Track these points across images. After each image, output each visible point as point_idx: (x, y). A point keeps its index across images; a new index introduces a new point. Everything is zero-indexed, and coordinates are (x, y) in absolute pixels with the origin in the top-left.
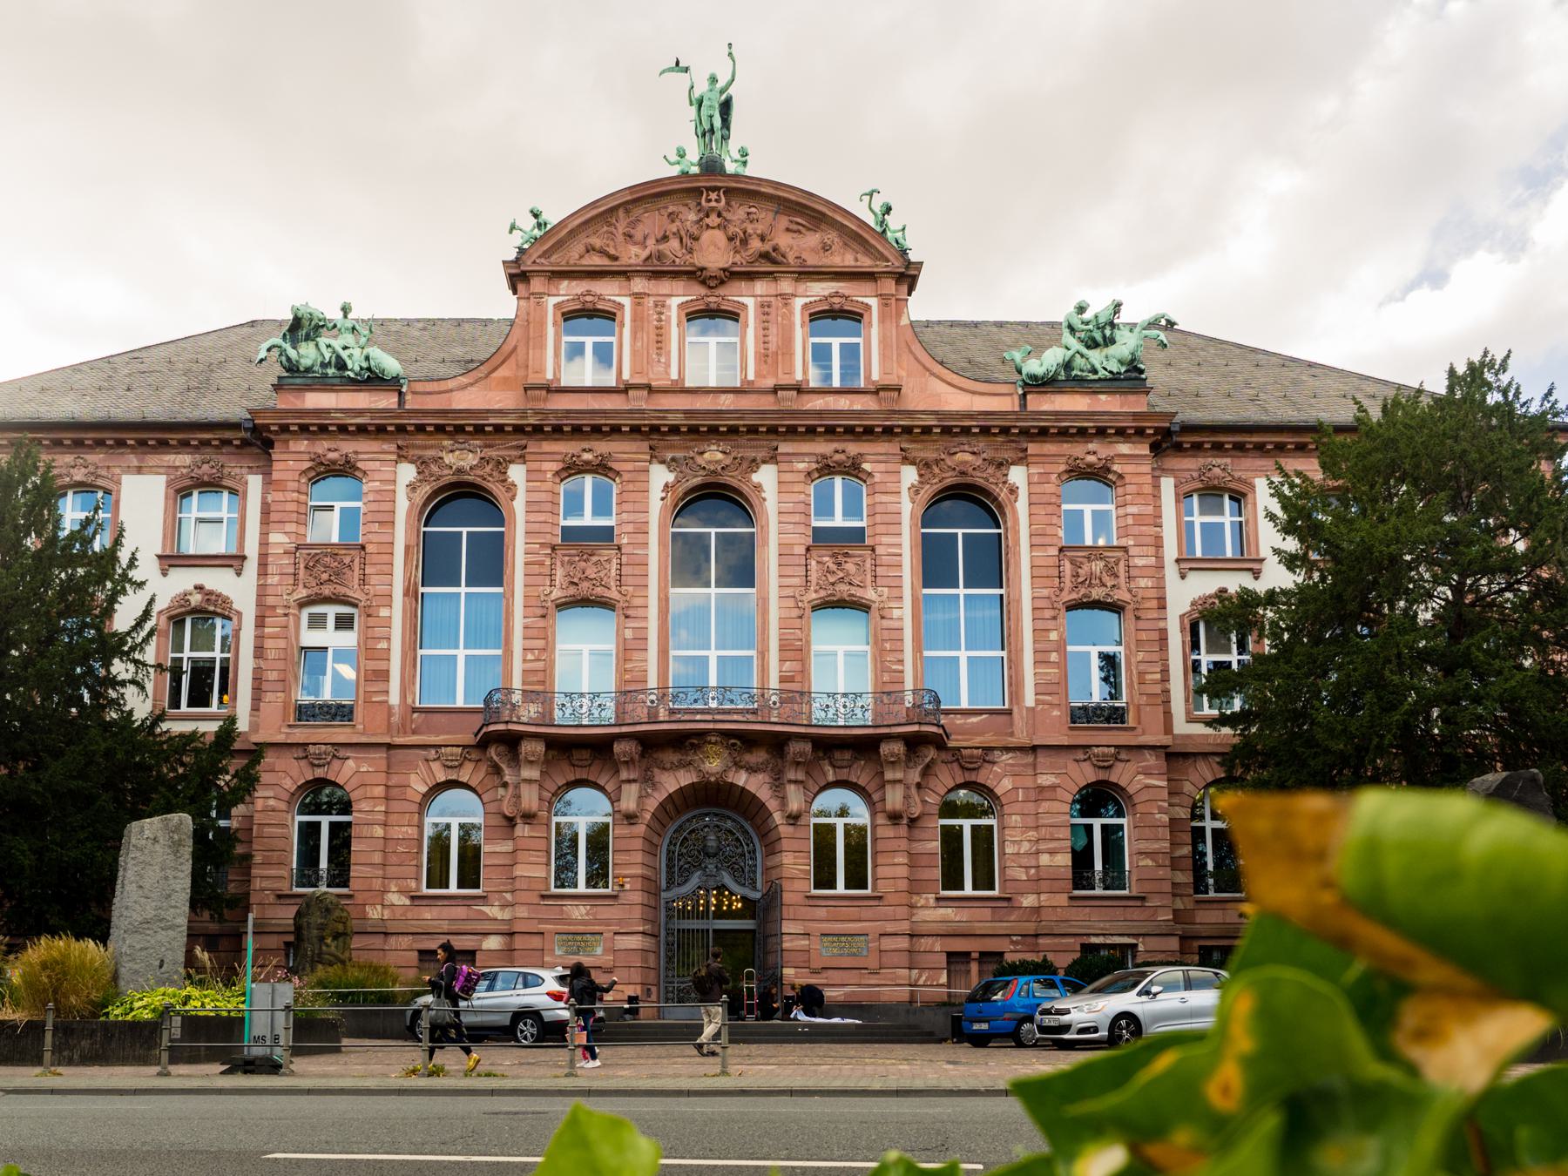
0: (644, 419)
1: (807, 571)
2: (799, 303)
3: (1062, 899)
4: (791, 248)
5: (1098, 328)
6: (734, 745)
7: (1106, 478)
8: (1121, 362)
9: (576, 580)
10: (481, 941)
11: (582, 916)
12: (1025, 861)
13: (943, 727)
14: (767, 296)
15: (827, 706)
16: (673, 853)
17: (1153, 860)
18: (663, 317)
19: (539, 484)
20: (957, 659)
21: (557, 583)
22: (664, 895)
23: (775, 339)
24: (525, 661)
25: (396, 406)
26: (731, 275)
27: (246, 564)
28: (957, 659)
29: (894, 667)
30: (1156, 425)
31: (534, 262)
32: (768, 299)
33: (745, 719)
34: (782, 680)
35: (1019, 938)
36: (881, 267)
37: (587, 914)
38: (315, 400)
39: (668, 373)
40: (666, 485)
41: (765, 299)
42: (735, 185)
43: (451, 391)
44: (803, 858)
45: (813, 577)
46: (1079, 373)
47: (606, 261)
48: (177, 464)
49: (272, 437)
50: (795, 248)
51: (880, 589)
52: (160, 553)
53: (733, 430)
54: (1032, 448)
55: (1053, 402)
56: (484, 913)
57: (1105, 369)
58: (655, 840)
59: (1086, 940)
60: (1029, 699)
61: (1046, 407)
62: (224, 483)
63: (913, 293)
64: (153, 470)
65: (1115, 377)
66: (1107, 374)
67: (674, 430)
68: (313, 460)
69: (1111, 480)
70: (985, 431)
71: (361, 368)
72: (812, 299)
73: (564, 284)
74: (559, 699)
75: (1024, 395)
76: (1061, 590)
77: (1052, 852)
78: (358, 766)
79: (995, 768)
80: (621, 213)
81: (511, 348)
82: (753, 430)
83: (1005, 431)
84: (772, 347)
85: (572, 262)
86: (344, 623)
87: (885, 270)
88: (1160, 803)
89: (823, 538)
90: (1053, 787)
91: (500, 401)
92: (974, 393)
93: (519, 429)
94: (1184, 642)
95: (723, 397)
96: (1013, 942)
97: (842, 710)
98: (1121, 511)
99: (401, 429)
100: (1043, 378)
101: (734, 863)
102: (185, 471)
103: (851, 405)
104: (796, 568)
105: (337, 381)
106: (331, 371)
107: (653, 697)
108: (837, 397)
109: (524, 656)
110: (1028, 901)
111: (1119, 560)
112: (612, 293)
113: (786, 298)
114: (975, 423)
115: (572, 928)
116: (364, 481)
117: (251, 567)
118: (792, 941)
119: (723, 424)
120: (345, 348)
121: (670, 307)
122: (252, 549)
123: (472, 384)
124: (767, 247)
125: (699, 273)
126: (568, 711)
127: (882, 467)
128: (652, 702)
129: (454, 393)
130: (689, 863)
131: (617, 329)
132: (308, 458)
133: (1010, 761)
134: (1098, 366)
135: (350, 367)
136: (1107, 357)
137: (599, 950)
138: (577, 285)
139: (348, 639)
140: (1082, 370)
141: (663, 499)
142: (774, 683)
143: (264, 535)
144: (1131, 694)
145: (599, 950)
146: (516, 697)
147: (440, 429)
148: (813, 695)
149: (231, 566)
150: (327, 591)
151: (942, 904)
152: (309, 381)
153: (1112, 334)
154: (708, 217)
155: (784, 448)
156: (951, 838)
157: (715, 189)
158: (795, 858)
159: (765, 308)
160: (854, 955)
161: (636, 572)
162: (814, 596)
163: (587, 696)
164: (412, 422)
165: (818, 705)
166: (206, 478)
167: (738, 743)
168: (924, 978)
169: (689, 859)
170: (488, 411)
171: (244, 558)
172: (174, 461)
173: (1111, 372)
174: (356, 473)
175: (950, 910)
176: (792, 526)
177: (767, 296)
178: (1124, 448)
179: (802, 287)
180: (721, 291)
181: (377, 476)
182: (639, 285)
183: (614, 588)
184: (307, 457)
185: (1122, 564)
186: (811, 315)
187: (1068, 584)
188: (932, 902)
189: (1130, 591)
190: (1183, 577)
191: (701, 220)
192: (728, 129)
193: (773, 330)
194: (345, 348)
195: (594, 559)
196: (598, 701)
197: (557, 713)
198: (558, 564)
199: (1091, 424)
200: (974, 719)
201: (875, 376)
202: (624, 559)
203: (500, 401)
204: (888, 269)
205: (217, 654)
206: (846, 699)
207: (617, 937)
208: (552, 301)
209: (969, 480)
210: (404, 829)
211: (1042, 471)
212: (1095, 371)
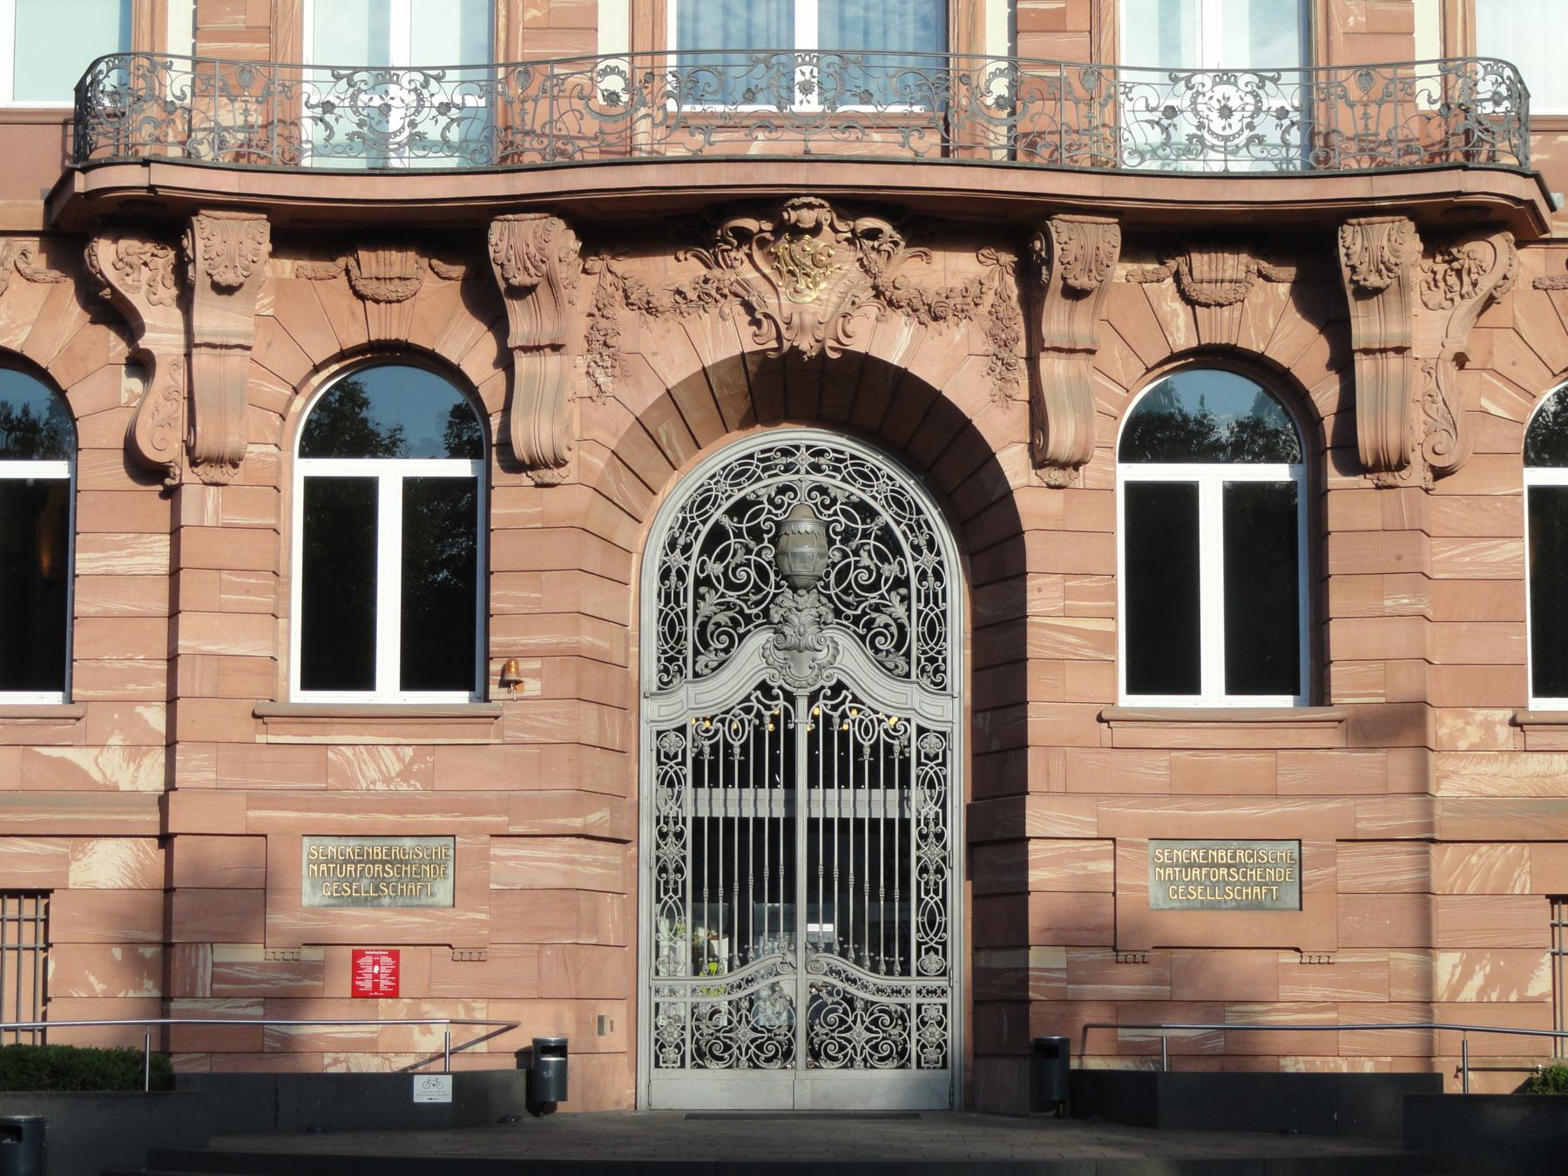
6: (873, 234)
10: (65, 861)
11: (387, 780)
13: (1537, 177)
15: (1171, 112)
16: (681, 576)
22: (650, 709)
33: (907, 154)
37: (405, 775)
44: (1093, 595)
56: (74, 769)
74: (315, 88)
97: (1217, 124)
101: (877, 608)
107: (615, 83)
115: (355, 819)
126: (345, 125)
128: (612, 97)
130: (728, 607)
137: (443, 891)
145: (443, 891)
146: (178, 82)
148: (1124, 76)
151: (1535, 738)
160: (1256, 906)
163: (405, 78)
165: (1141, 105)
167: (886, 228)
168: (1478, 980)
169: (732, 597)
196: (440, 93)
197: (310, 131)
206: (1228, 90)
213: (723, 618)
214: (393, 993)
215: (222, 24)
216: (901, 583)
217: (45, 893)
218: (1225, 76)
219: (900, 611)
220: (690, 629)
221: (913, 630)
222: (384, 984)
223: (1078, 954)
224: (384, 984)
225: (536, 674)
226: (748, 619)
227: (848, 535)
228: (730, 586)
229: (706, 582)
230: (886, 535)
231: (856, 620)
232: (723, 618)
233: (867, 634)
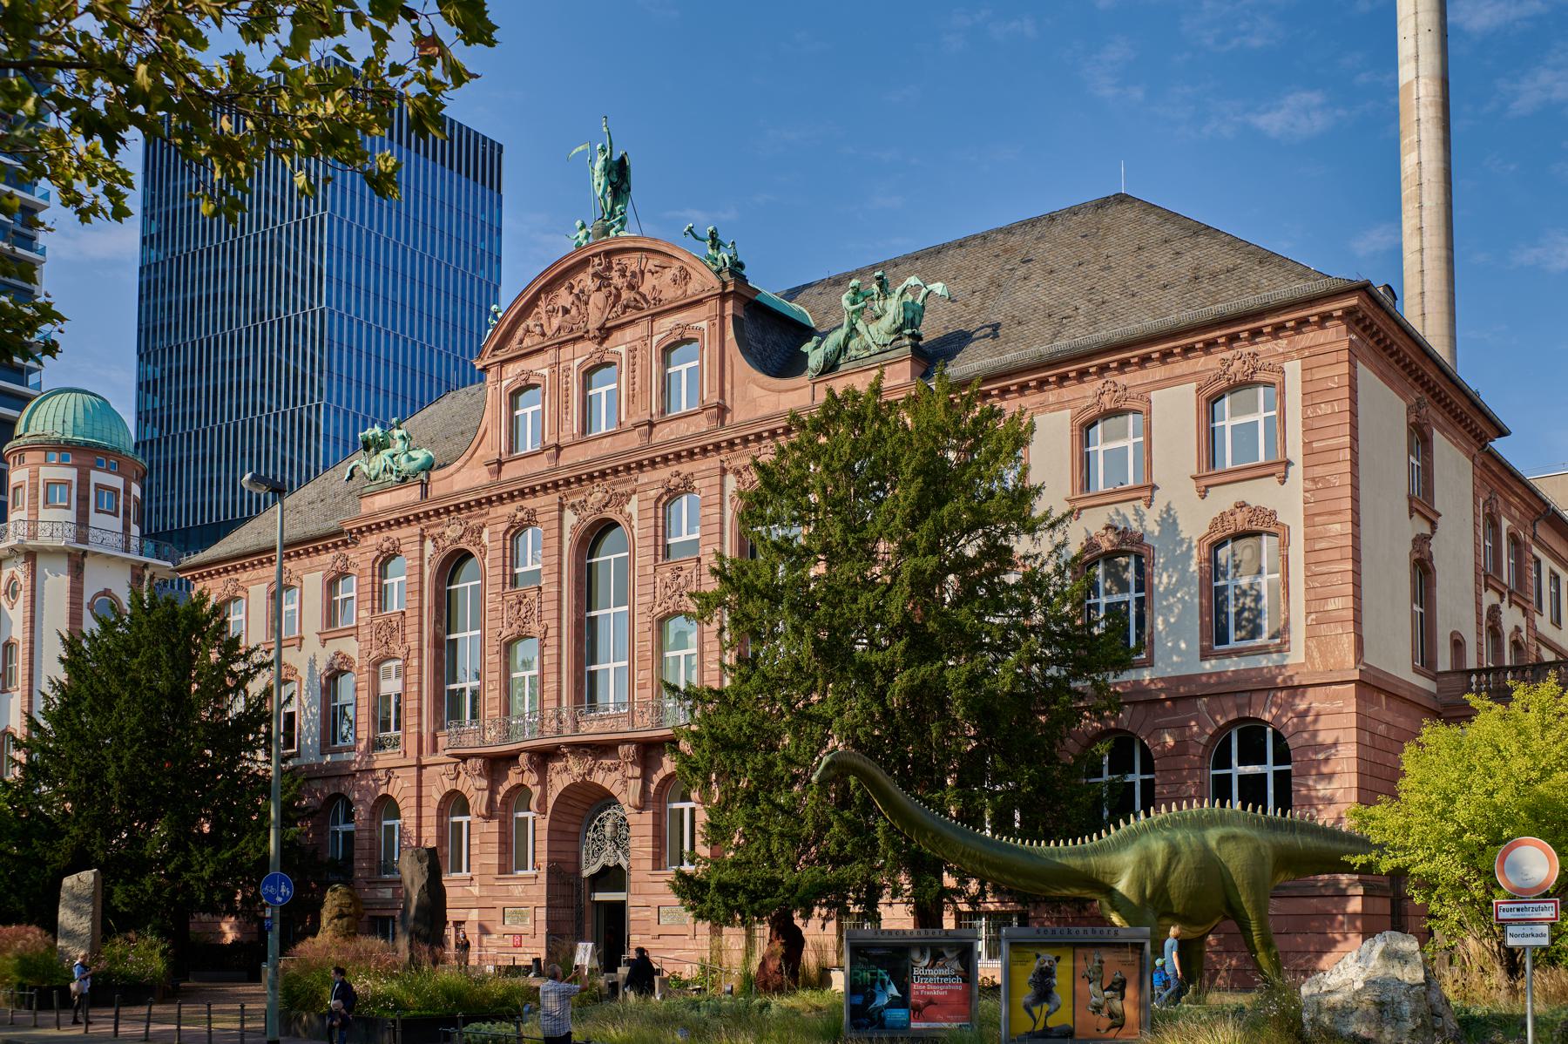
38: (382, 501)
123: (462, 466)
182: (549, 356)
212: (867, 348)
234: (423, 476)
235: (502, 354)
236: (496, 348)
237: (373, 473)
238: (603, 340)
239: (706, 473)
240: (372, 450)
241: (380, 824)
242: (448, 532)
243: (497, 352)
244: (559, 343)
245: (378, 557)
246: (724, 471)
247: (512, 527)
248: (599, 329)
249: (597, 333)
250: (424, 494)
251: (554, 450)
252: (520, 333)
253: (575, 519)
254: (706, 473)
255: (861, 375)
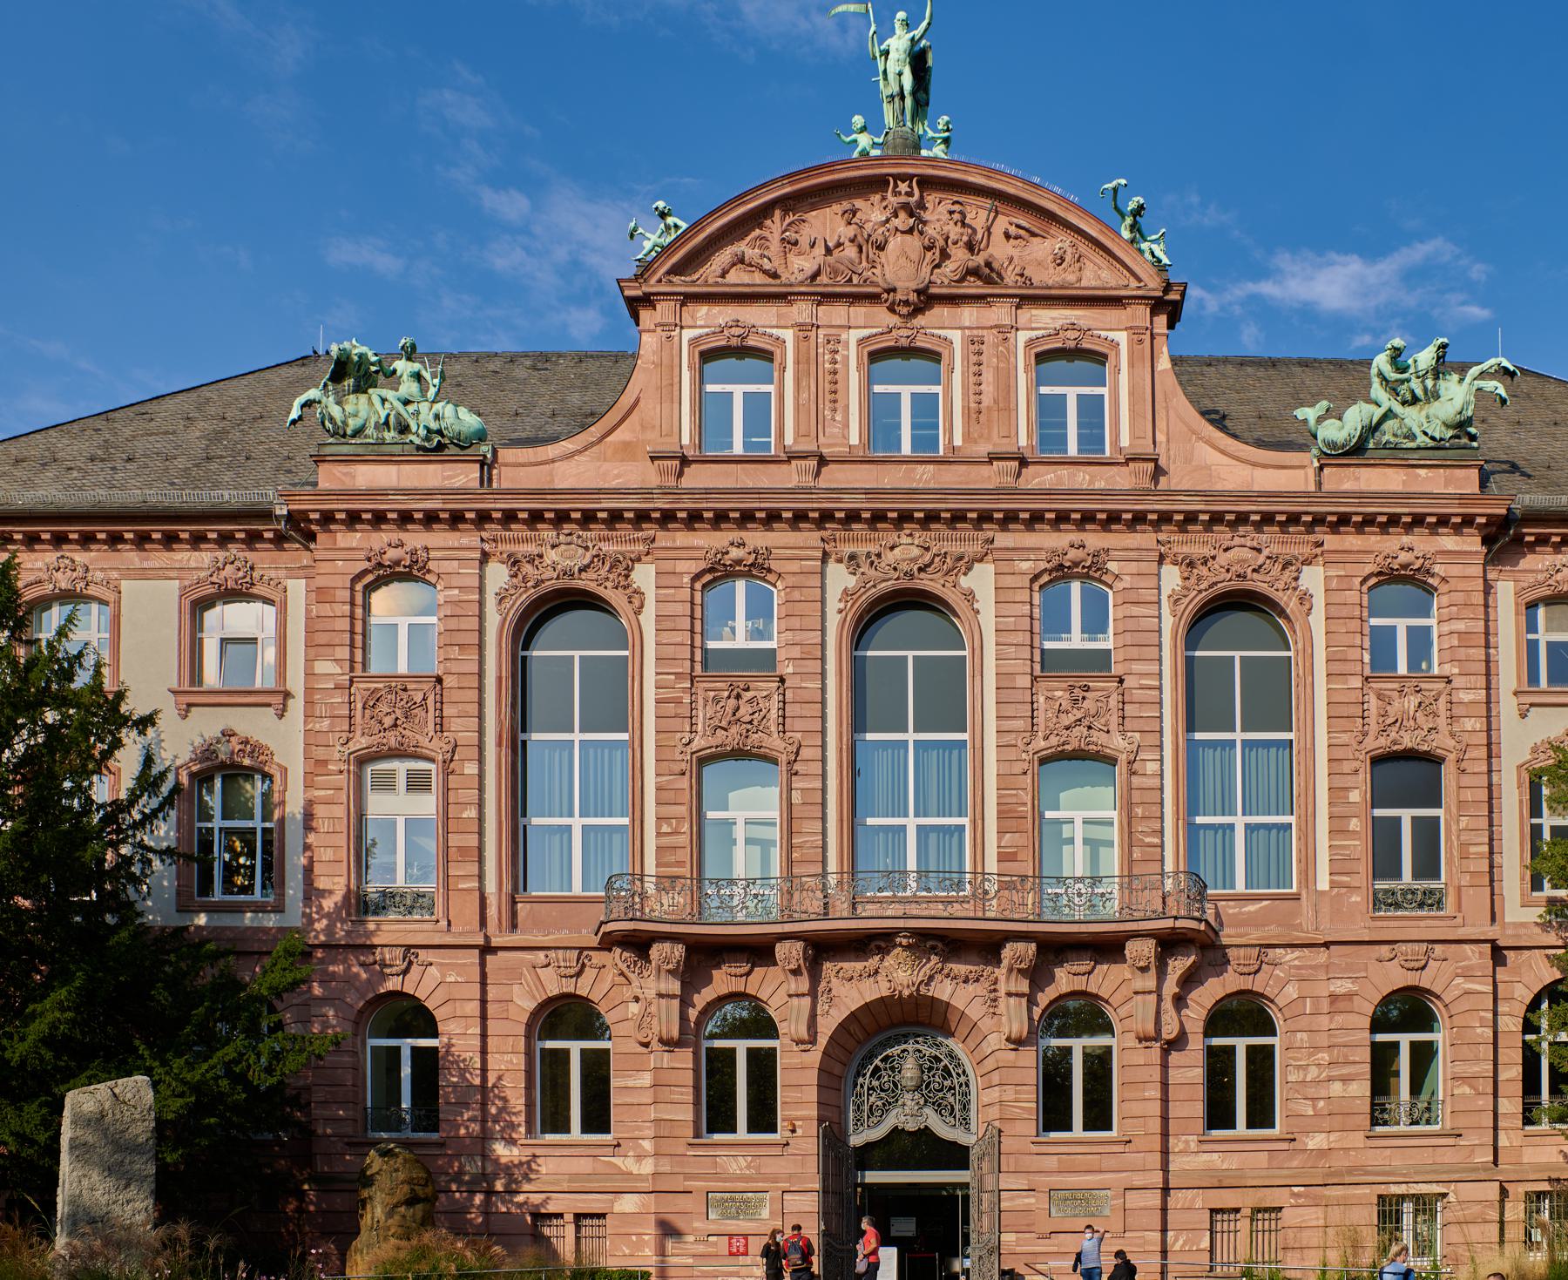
0: (811, 501)
1: (1033, 711)
2: (1023, 337)
3: (1358, 1139)
4: (1011, 260)
5: (1418, 377)
7: (1425, 582)
8: (1447, 426)
9: (724, 724)
12: (1311, 1092)
14: (978, 328)
17: (1471, 1087)
18: (838, 357)
19: (672, 591)
20: (1231, 827)
21: (700, 727)
23: (991, 388)
24: (659, 834)
25: (477, 484)
26: (926, 300)
27: (290, 702)
28: (1231, 827)
29: (1147, 840)
30: (1489, 511)
31: (660, 281)
32: (980, 332)
34: (1002, 858)
35: (1302, 1189)
36: (1132, 289)
37: (748, 1167)
38: (368, 476)
39: (846, 437)
40: (845, 591)
41: (975, 332)
42: (930, 172)
43: (553, 461)
45: (1041, 719)
46: (1392, 439)
47: (759, 278)
48: (193, 564)
49: (313, 527)
50: (1016, 261)
51: (1129, 734)
52: (175, 686)
53: (932, 517)
54: (1331, 541)
55: (1357, 479)
57: (1425, 434)
58: (837, 1069)
59: (1382, 1190)
60: (1323, 883)
61: (1347, 486)
62: (255, 590)
63: (1177, 325)
64: (161, 574)
65: (1438, 445)
66: (1428, 440)
67: (853, 516)
68: (369, 559)
69: (1432, 586)
70: (1268, 519)
71: (429, 430)
72: (1040, 333)
73: (703, 311)
75: (1321, 468)
76: (1365, 734)
77: (1345, 1080)
78: (443, 975)
79: (1277, 972)
80: (778, 213)
81: (632, 401)
82: (958, 517)
83: (1294, 519)
84: (987, 400)
85: (711, 281)
86: (417, 783)
87: (1135, 293)
88: (1482, 1014)
89: (1051, 663)
90: (1350, 996)
91: (618, 476)
92: (1255, 464)
93: (642, 517)
94: (1521, 802)
95: (920, 468)
96: (1294, 1195)
97: (1077, 900)
98: (1446, 628)
99: (483, 518)
100: (1344, 446)
102: (203, 574)
103: (1091, 482)
104: (1019, 706)
105: (397, 449)
106: (390, 436)
108: (1072, 469)
109: (658, 827)
110: (1316, 1142)
111: (1439, 694)
112: (768, 323)
113: (1005, 332)
114: (1254, 508)
115: (728, 1186)
116: (439, 587)
117: (297, 706)
118: (1012, 1199)
119: (920, 506)
120: (406, 402)
121: (847, 343)
122: (296, 682)
123: (580, 452)
124: (979, 260)
125: (885, 295)
127: (1133, 568)
129: (557, 464)
131: (776, 374)
132: (363, 557)
133: (1296, 963)
134: (1417, 431)
135: (414, 429)
136: (1428, 417)
137: (765, 1213)
138: (720, 313)
139: (427, 805)
140: (1395, 435)
141: (840, 611)
142: (992, 865)
143: (309, 661)
144: (1449, 872)
147: (536, 517)
149: (269, 705)
150: (392, 740)
152: (360, 450)
153: (1435, 385)
154: (896, 217)
155: (1003, 539)
156: (1218, 1063)
157: (909, 177)
158: (1017, 1092)
159: (975, 343)
161: (804, 713)
162: (1043, 744)
164: (498, 506)
166: (230, 584)
167: (940, 945)
169: (883, 1094)
170: (600, 491)
171: (287, 695)
172: (189, 560)
173: (1433, 438)
174: (428, 577)
175: (1215, 1156)
176: (1013, 649)
177: (978, 328)
178: (1448, 542)
179: (1026, 315)
180: (919, 321)
181: (456, 581)
182: (802, 311)
183: (776, 735)
184: (362, 555)
185: (1443, 700)
186: (1038, 355)
187: (1373, 728)
188: (1193, 1146)
189: (1452, 735)
190: (1523, 716)
191: (887, 221)
192: (926, 91)
193: (988, 376)
194: (406, 402)
195: (749, 695)
198: (701, 702)
199: (1406, 510)
200: (1252, 907)
201: (1125, 441)
202: (789, 694)
203: (618, 476)
204: (1140, 293)
205: (257, 823)
206: (1081, 886)
207: (786, 1196)
208: (688, 334)
209: (1247, 585)
210: (507, 1057)
211: (1343, 573)
212: (1411, 436)
213: (879, 1103)
214: (746, 1254)
215: (666, 860)
216: (952, 1088)
217: (602, 1216)
218: (1080, 879)
219: (951, 1100)
220: (866, 1108)
221: (957, 1107)
222: (741, 1250)
223: (1020, 1235)
224: (741, 1250)
225: (801, 1127)
226: (890, 1104)
227: (930, 1069)
228: (882, 1090)
229: (873, 1089)
230: (946, 1068)
231: (934, 1104)
232: (879, 1103)
233: (939, 1107)
234: (485, 449)
235: (680, 284)
236: (676, 270)
237: (353, 424)
238: (918, 310)
239: (1132, 554)
240: (349, 382)
241: (364, 1044)
242: (551, 556)
243: (676, 279)
244: (823, 295)
245: (365, 572)
246: (1161, 559)
247: (711, 570)
248: (919, 292)
249: (913, 297)
250: (486, 479)
251: (813, 463)
252: (724, 257)
253: (851, 582)
254: (1132, 554)
255: (1401, 471)
